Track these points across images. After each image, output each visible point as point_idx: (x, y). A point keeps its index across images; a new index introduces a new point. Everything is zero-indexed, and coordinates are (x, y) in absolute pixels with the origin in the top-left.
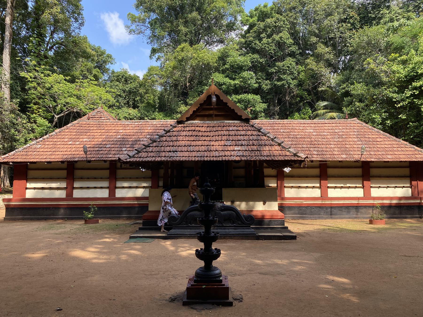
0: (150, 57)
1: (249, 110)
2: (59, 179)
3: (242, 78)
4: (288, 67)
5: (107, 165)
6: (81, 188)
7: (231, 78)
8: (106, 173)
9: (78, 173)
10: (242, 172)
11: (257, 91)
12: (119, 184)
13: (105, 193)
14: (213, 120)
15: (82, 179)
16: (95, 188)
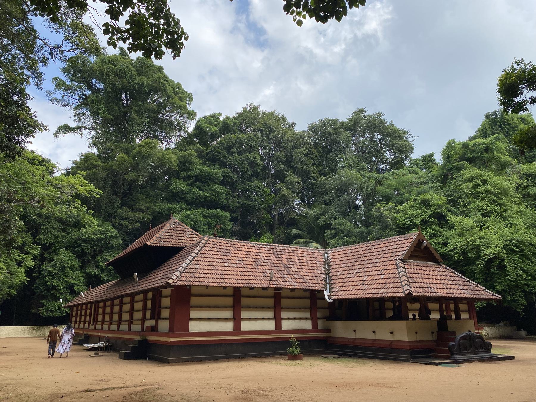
0: (56, 134)
1: (218, 227)
2: (226, 307)
3: (213, 190)
4: (259, 188)
5: (308, 294)
6: (250, 319)
7: (200, 190)
8: (271, 302)
9: (244, 301)
10: (377, 305)
11: (225, 208)
12: (284, 314)
13: (270, 325)
14: (419, 260)
15: (249, 308)
16: (263, 319)
